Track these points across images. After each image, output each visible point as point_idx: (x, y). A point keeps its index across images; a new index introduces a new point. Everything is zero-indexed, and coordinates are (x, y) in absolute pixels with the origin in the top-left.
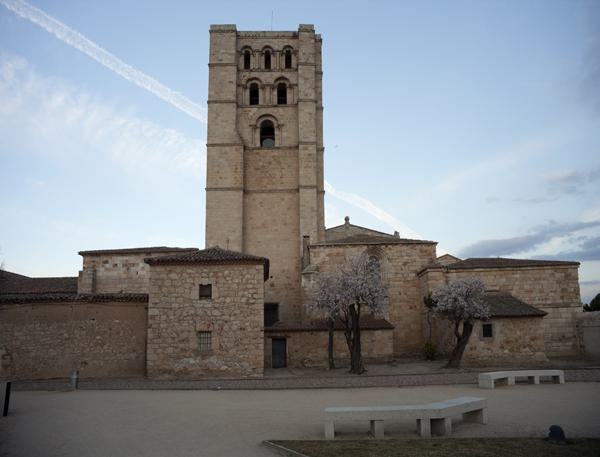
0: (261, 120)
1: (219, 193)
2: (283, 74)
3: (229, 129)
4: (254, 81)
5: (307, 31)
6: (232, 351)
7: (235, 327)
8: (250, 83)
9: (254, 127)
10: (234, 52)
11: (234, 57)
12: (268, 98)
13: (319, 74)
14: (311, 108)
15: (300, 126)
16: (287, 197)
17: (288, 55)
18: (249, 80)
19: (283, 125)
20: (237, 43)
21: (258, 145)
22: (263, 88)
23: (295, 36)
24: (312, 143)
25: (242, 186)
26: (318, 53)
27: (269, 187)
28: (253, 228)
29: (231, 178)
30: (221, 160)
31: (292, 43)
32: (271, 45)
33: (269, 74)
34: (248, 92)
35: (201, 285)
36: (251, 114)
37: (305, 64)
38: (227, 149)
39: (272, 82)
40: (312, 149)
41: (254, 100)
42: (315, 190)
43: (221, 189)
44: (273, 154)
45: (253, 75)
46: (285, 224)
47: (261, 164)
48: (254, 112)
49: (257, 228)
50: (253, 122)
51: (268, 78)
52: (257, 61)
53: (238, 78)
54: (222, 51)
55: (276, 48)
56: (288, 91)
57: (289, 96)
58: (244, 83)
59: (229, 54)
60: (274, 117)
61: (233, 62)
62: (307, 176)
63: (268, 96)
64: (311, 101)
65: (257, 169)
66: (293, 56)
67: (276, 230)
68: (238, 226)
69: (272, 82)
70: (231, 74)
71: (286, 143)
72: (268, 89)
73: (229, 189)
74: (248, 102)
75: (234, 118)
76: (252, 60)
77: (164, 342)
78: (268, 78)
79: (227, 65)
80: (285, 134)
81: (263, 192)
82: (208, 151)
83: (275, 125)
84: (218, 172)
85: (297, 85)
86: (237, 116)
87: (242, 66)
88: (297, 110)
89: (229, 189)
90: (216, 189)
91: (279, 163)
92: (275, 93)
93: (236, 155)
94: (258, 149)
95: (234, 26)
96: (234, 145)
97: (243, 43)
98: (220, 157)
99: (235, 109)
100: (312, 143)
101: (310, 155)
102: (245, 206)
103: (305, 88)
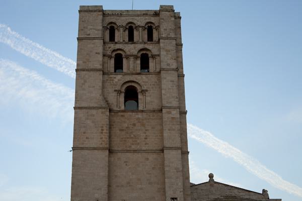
1: (86, 152)
2: (147, 46)
3: (95, 96)
5: (167, 11)
9: (119, 92)
10: (101, 28)
11: (100, 32)
12: (131, 67)
13: (179, 45)
14: (173, 76)
15: (163, 92)
16: (152, 157)
17: (150, 29)
18: (114, 51)
19: (147, 91)
21: (123, 108)
22: (127, 57)
23: (156, 14)
24: (175, 108)
25: (108, 146)
26: (178, 28)
27: (133, 147)
28: (118, 186)
29: (97, 139)
30: (89, 122)
31: (153, 20)
32: (135, 22)
33: (132, 46)
34: (113, 61)
36: (116, 80)
37: (167, 38)
38: (94, 112)
39: (135, 52)
40: (175, 113)
42: (180, 151)
43: (87, 149)
44: (137, 116)
45: (118, 46)
46: (150, 183)
47: (126, 125)
48: (119, 79)
49: (122, 186)
50: (118, 88)
51: (132, 49)
52: (121, 35)
53: (104, 49)
54: (90, 27)
56: (151, 60)
58: (109, 53)
59: (97, 28)
60: (137, 83)
61: (100, 36)
62: (170, 138)
63: (131, 65)
64: (173, 70)
65: (121, 130)
66: (154, 31)
67: (141, 189)
68: (104, 184)
71: (150, 107)
72: (132, 59)
73: (94, 149)
74: (112, 70)
75: (100, 84)
76: (117, 34)
78: (132, 49)
79: (94, 38)
80: (148, 99)
81: (128, 151)
82: (75, 113)
83: (139, 90)
84: (84, 133)
85: (159, 55)
86: (103, 82)
87: (107, 38)
88: (160, 80)
89: (94, 149)
90: (82, 149)
91: (143, 125)
92: (139, 62)
93: (102, 117)
94: (123, 111)
95: (102, 6)
96: (100, 108)
97: (109, 20)
98: (87, 119)
99: (101, 77)
100: (175, 108)
102: (110, 165)
103: (166, 59)
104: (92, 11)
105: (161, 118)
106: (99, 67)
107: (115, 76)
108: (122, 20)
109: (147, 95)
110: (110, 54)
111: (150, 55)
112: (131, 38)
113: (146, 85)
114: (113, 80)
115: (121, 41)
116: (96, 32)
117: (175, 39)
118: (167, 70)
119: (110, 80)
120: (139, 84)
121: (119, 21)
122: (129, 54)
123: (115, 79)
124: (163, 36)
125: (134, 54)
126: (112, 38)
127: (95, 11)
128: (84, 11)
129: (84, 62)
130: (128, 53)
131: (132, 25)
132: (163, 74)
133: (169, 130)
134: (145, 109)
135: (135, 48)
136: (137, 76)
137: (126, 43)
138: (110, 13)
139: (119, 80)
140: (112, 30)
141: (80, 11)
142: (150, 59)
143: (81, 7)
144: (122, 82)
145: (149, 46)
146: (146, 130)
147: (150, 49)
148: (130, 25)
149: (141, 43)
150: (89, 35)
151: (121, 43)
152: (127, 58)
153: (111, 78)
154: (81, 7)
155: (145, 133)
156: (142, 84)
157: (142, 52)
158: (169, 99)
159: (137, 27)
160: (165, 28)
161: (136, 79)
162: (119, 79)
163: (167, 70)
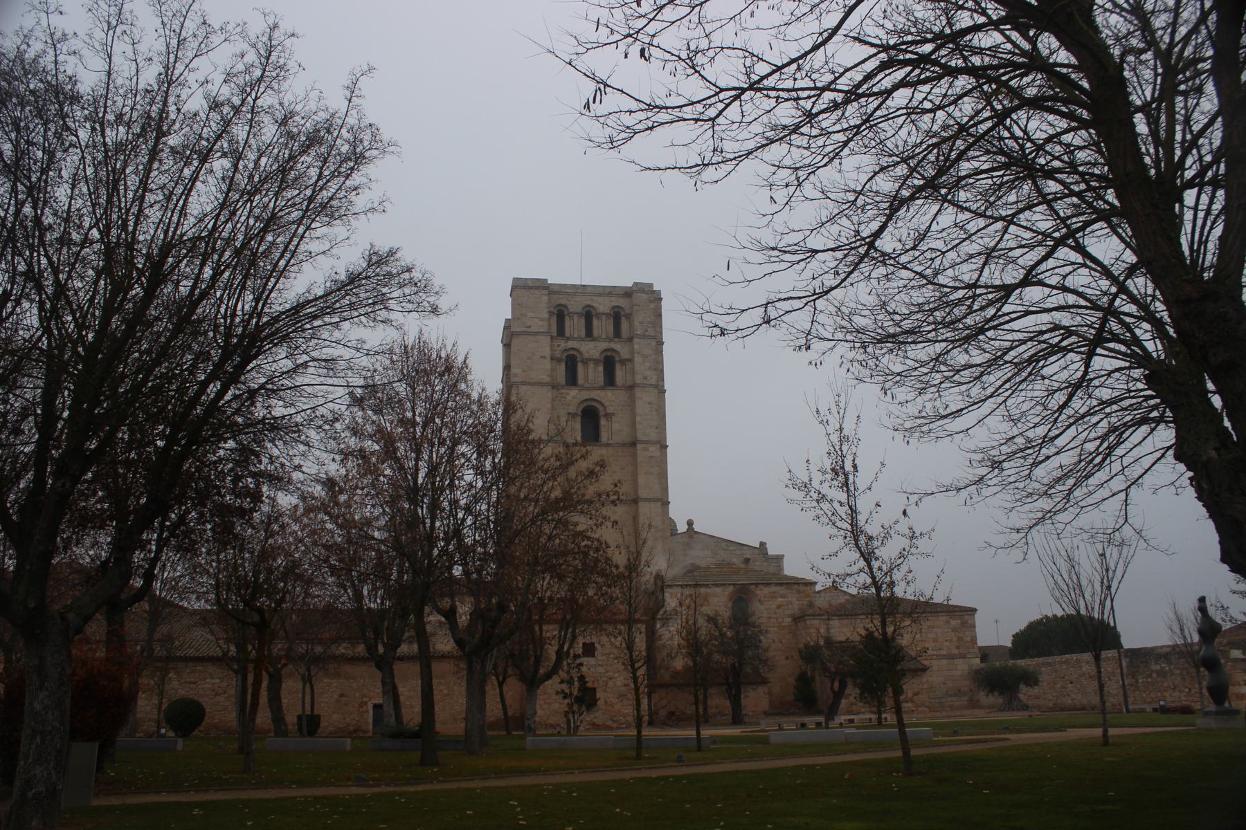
2: (612, 345)
4: (572, 352)
5: (643, 292)
7: (619, 684)
8: (565, 354)
10: (546, 316)
11: (545, 323)
12: (591, 377)
15: (638, 419)
18: (566, 350)
19: (613, 414)
22: (585, 362)
23: (627, 293)
24: (654, 443)
31: (621, 302)
33: (591, 345)
35: (584, 644)
36: (569, 398)
37: (644, 336)
39: (597, 355)
41: (572, 380)
42: (659, 504)
45: (571, 344)
48: (574, 396)
50: (572, 409)
51: (592, 349)
52: (575, 326)
53: (552, 350)
55: (601, 309)
56: (618, 366)
57: (619, 373)
58: (558, 354)
59: (540, 320)
64: (652, 386)
66: (623, 319)
69: (597, 355)
70: (543, 346)
71: (617, 439)
72: (591, 366)
74: (562, 380)
75: (549, 406)
80: (616, 426)
83: (602, 413)
85: (631, 360)
92: (601, 369)
100: (654, 443)
101: (651, 457)
103: (642, 368)
104: (531, 288)
105: (634, 456)
106: (547, 379)
111: (617, 359)
115: (576, 336)
116: (540, 323)
118: (644, 386)
126: (561, 332)
127: (537, 288)
128: (521, 288)
129: (524, 371)
130: (586, 355)
132: (639, 393)
133: (646, 474)
134: (610, 442)
137: (582, 340)
138: (556, 289)
139: (574, 398)
140: (560, 315)
141: (514, 288)
145: (617, 346)
149: (605, 340)
150: (530, 327)
154: (515, 280)
156: (607, 404)
157: (605, 354)
158: (645, 431)
159: (598, 315)
162: (574, 396)
163: (644, 386)
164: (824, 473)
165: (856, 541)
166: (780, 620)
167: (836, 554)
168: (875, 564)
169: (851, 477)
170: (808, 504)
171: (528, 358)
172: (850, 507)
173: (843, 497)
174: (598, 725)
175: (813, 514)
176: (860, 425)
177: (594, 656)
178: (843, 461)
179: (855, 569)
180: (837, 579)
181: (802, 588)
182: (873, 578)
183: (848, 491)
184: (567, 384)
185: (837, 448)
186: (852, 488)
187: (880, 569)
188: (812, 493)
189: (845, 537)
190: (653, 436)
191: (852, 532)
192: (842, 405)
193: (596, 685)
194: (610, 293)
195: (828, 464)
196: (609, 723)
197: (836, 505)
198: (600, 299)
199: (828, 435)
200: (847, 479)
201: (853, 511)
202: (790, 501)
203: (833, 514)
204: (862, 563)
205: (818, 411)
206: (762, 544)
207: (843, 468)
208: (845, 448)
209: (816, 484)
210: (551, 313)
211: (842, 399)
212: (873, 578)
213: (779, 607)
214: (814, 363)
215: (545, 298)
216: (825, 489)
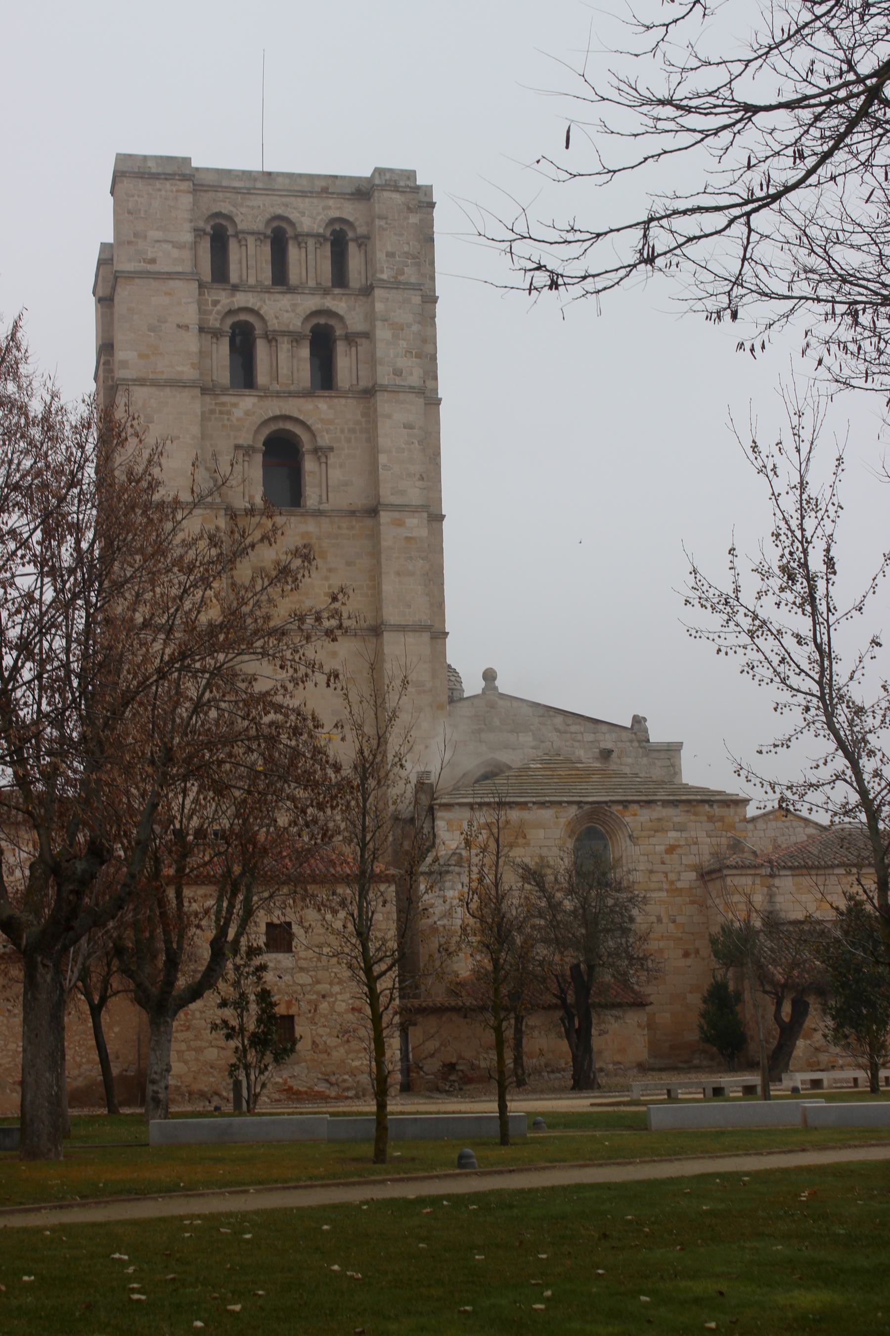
0: (266, 432)
2: (330, 303)
4: (243, 317)
5: (396, 189)
6: (339, 1054)
7: (341, 1007)
8: (229, 321)
10: (189, 237)
11: (187, 254)
12: (284, 370)
15: (383, 459)
18: (230, 312)
19: (331, 449)
20: (195, 203)
22: (271, 338)
24: (415, 510)
31: (349, 211)
32: (294, 216)
36: (238, 413)
37: (396, 285)
39: (296, 323)
42: (426, 637)
45: (242, 299)
50: (245, 439)
54: (154, 234)
56: (341, 348)
58: (214, 322)
60: (303, 424)
64: (412, 389)
66: (352, 248)
69: (296, 323)
71: (339, 500)
72: (285, 346)
74: (223, 376)
75: (196, 430)
77: (197, 1037)
80: (335, 474)
83: (307, 446)
85: (367, 335)
92: (305, 352)
100: (415, 510)
101: (408, 539)
104: (155, 176)
105: (374, 536)
106: (188, 372)
107: (234, 400)
108: (253, 208)
109: (331, 461)
110: (218, 325)
111: (338, 332)
112: (280, 276)
113: (328, 431)
114: (229, 413)
115: (252, 281)
116: (175, 253)
117: (416, 287)
118: (394, 390)
119: (221, 413)
120: (308, 428)
121: (243, 210)
122: (277, 327)
123: (234, 410)
124: (384, 276)
125: (291, 328)
126: (220, 273)
127: (168, 177)
129: (142, 356)
130: (274, 324)
131: (284, 225)
132: (383, 403)
133: (398, 574)
134: (325, 507)
135: (294, 306)
136: (301, 400)
139: (247, 413)
141: (118, 177)
142: (339, 343)
143: (118, 155)
144: (257, 420)
145: (338, 304)
146: (330, 570)
147: (341, 312)
148: (275, 224)
149: (313, 292)
150: (153, 261)
151: (251, 289)
152: (269, 341)
153: (223, 404)
154: (122, 159)
155: (327, 578)
156: (317, 426)
157: (315, 321)
160: (389, 249)
161: (299, 411)
163: (394, 390)
164: (765, 575)
165: (830, 716)
166: (672, 876)
167: (786, 744)
168: (868, 765)
169: (821, 584)
170: (732, 640)
171: (152, 329)
172: (819, 647)
173: (804, 625)
174: (298, 1093)
175: (740, 660)
176: (841, 476)
177: (289, 949)
178: (805, 552)
179: (825, 773)
180: (788, 794)
181: (717, 810)
182: (863, 792)
183: (814, 613)
184: (234, 385)
185: (794, 523)
186: (823, 608)
187: (877, 774)
188: (740, 618)
189: (807, 709)
190: (414, 495)
191: (822, 698)
192: (806, 435)
193: (293, 1011)
194: (325, 190)
195: (773, 557)
196: (321, 1087)
197: (789, 642)
198: (303, 204)
199: (775, 496)
200: (812, 589)
201: (824, 653)
202: (694, 633)
203: (782, 661)
204: (841, 763)
205: (755, 447)
206: (638, 721)
207: (805, 565)
208: (810, 524)
209: (748, 598)
210: (198, 232)
211: (807, 421)
212: (863, 792)
213: (671, 849)
214: (748, 346)
215: (186, 200)
216: (767, 610)
